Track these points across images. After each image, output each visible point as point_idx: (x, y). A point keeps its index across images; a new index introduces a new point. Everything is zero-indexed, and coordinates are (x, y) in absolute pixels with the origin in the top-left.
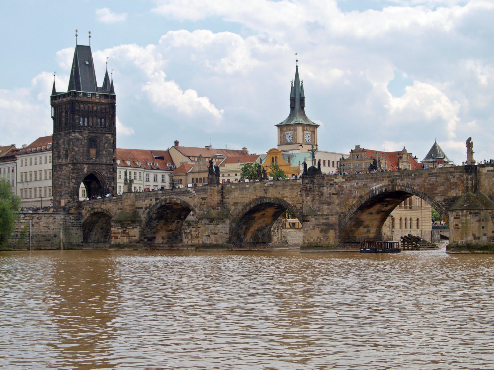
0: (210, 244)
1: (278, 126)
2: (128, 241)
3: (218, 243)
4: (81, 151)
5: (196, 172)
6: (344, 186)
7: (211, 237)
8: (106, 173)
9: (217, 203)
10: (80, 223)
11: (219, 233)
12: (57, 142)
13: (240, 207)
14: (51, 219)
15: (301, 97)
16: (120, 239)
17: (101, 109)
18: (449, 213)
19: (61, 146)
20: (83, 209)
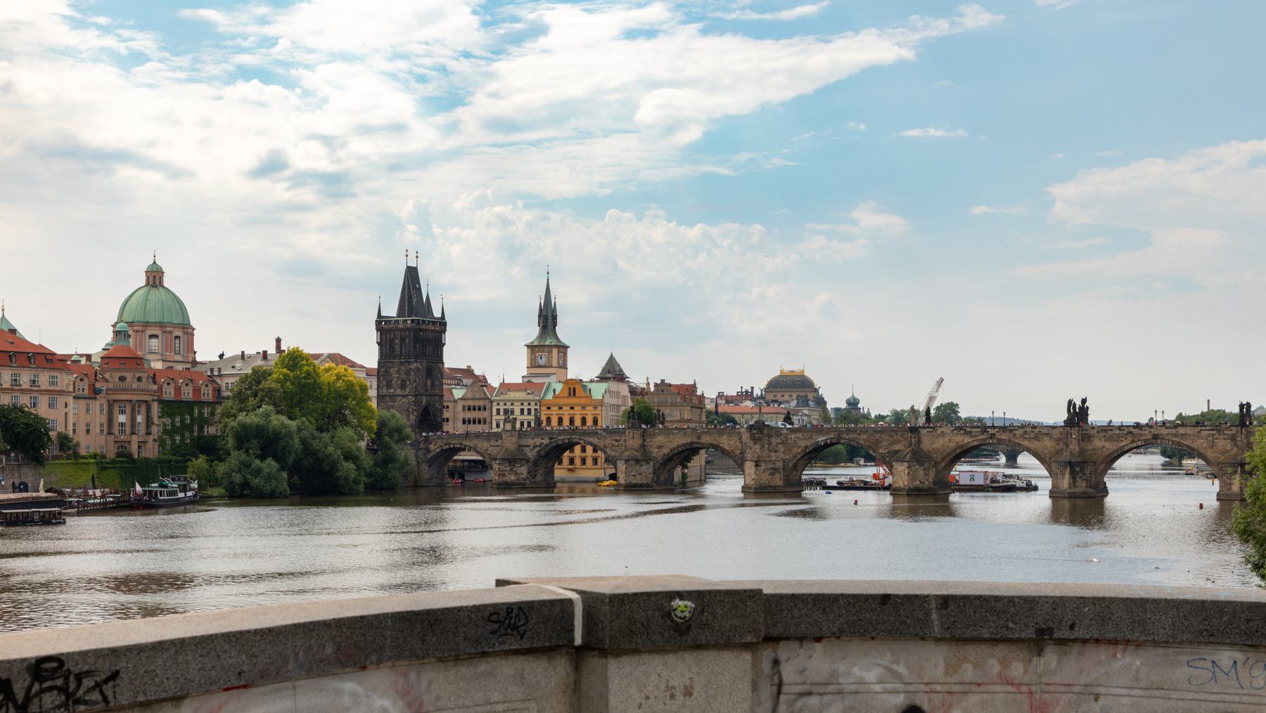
0: (636, 484)
1: (528, 346)
5: (469, 399)
11: (644, 474)
13: (666, 451)
15: (554, 314)
18: (894, 463)
20: (431, 443)
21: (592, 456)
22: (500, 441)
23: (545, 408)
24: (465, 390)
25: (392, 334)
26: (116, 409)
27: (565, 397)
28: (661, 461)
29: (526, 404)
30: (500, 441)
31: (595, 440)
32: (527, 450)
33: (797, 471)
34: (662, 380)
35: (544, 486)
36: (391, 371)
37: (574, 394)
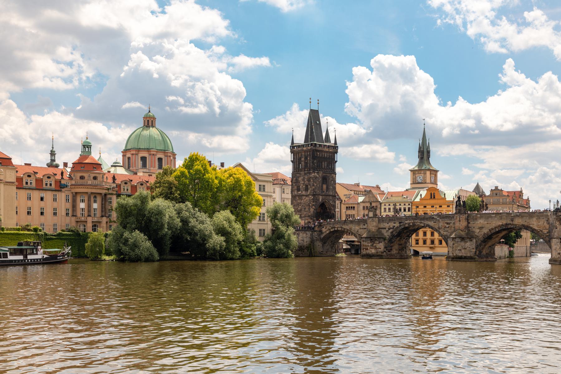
1: (411, 171)
4: (318, 186)
8: (332, 202)
13: (485, 231)
14: (305, 235)
15: (428, 150)
17: (329, 156)
20: (323, 227)
23: (415, 207)
24: (364, 197)
25: (300, 154)
26: (78, 198)
27: (428, 199)
28: (482, 239)
29: (402, 204)
30: (366, 225)
31: (431, 223)
32: (384, 231)
35: (398, 257)
36: (299, 179)
37: (434, 197)
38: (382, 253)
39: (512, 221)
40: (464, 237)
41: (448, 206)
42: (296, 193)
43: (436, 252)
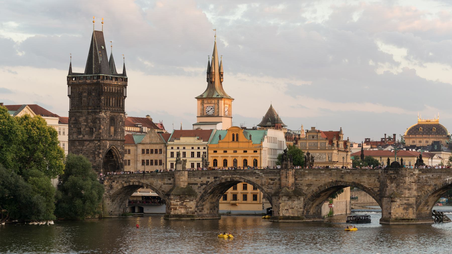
2: (185, 212)
3: (295, 216)
4: (106, 129)
5: (147, 144)
6: (421, 176)
7: (289, 211)
9: (291, 184)
10: (110, 194)
11: (295, 208)
12: (75, 118)
13: (314, 188)
15: (220, 72)
16: (178, 210)
17: (118, 91)
19: (82, 124)
20: (114, 181)
21: (251, 193)
22: (172, 180)
27: (229, 142)
29: (196, 148)
30: (172, 180)
32: (195, 188)
33: (428, 206)
34: (312, 128)
35: (209, 218)
37: (237, 140)
38: (193, 213)
39: (343, 178)
40: (291, 195)
41: (255, 151)
42: (75, 136)
43: (239, 209)
